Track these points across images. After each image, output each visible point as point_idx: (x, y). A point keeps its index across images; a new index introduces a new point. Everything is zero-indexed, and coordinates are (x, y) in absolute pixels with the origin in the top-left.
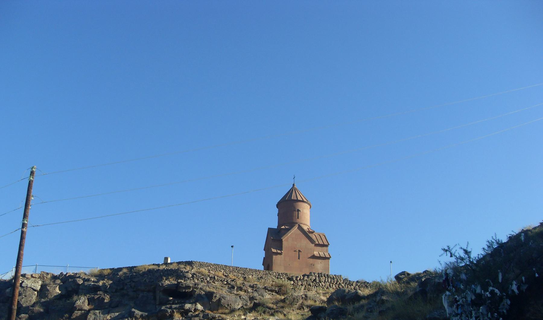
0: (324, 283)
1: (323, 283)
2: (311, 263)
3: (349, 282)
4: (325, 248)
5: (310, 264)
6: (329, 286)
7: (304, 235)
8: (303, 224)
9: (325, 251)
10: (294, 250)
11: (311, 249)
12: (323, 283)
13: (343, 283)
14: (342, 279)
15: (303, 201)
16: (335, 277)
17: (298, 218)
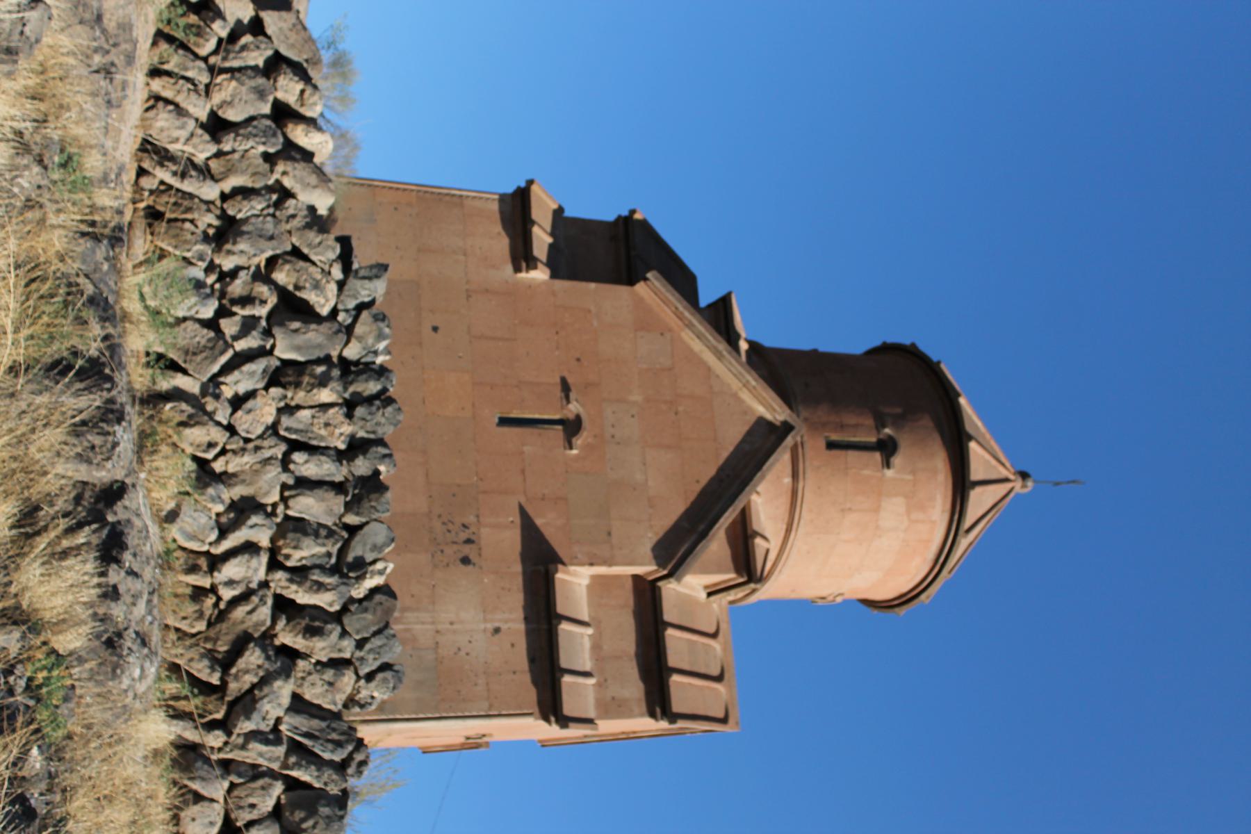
0: (273, 429)
1: (265, 410)
2: (485, 535)
3: (321, 795)
4: (634, 689)
5: (471, 519)
6: (237, 492)
7: (712, 471)
8: (794, 493)
9: (614, 690)
10: (570, 380)
11: (609, 534)
12: (265, 410)
13: (299, 704)
14: (350, 702)
15: (962, 485)
16: (359, 591)
17: (831, 445)
